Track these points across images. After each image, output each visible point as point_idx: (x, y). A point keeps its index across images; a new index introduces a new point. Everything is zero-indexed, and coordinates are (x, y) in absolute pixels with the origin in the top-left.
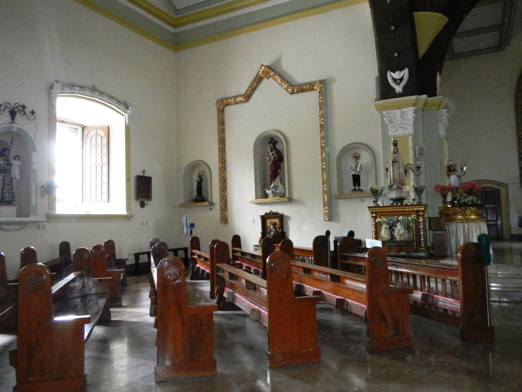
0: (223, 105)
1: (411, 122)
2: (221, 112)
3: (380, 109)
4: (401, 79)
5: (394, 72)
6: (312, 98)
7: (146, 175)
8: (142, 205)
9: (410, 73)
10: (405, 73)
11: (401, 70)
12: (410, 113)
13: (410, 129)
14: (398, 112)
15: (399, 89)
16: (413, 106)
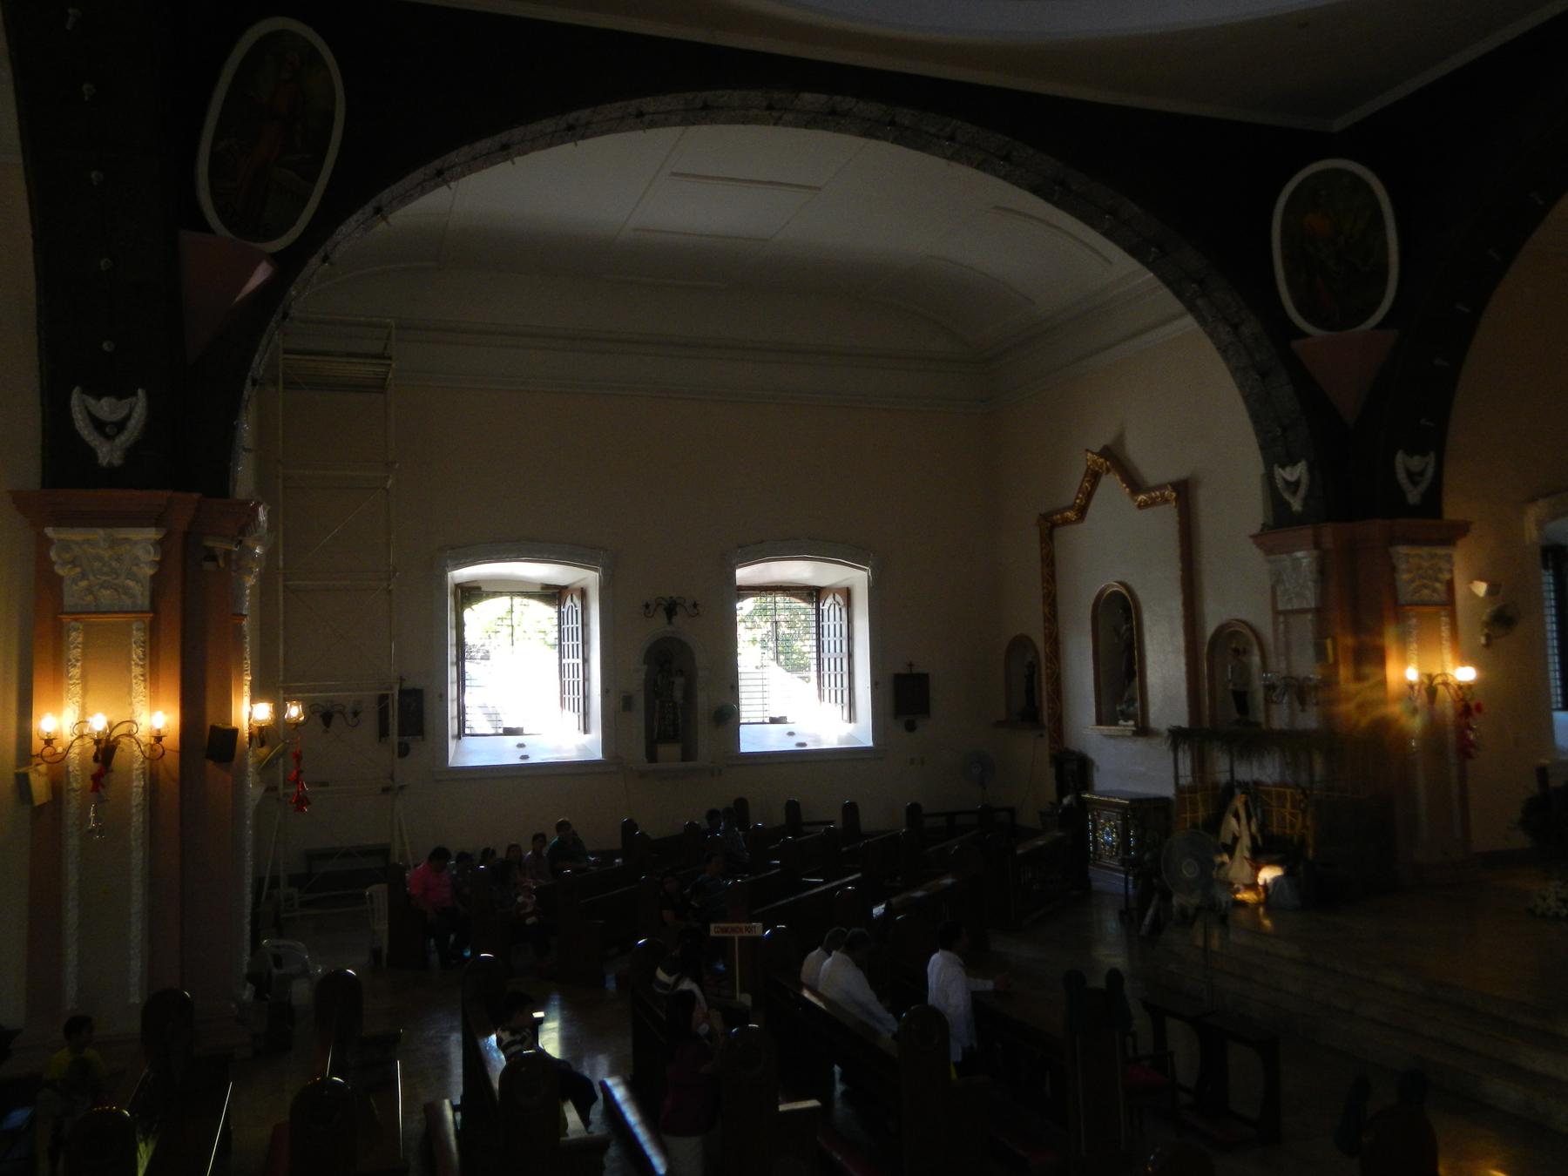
0: (1050, 526)
1: (1310, 584)
2: (1048, 538)
3: (1269, 551)
4: (1297, 484)
5: (1283, 467)
6: (1166, 517)
7: (915, 670)
8: (910, 727)
9: (1310, 469)
10: (1297, 472)
11: (1294, 463)
12: (1305, 557)
13: (1310, 601)
14: (1284, 556)
15: (1296, 505)
16: (1317, 545)
